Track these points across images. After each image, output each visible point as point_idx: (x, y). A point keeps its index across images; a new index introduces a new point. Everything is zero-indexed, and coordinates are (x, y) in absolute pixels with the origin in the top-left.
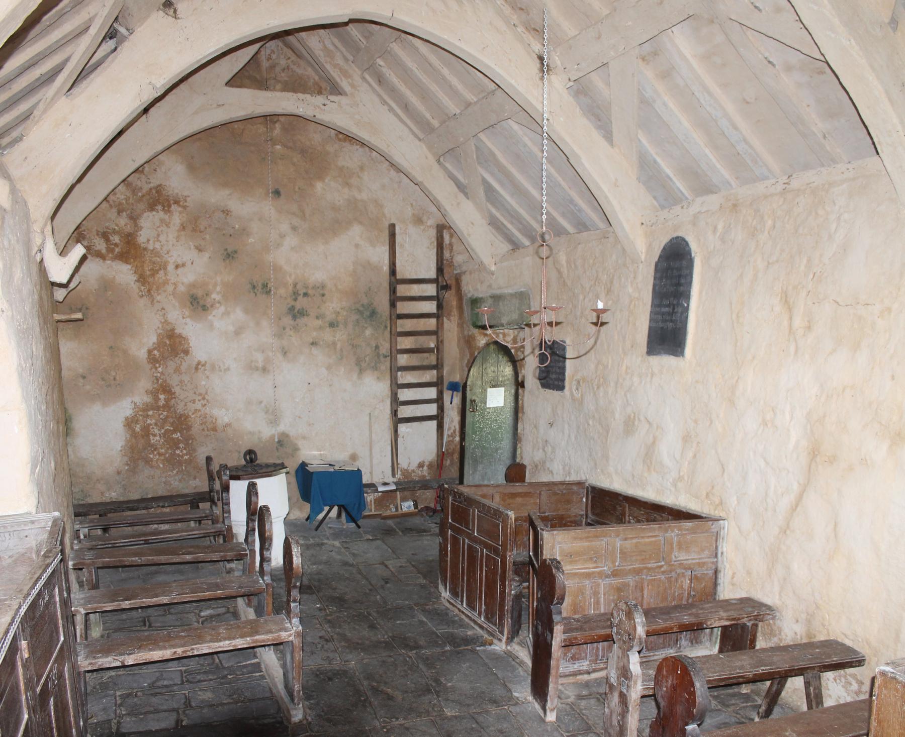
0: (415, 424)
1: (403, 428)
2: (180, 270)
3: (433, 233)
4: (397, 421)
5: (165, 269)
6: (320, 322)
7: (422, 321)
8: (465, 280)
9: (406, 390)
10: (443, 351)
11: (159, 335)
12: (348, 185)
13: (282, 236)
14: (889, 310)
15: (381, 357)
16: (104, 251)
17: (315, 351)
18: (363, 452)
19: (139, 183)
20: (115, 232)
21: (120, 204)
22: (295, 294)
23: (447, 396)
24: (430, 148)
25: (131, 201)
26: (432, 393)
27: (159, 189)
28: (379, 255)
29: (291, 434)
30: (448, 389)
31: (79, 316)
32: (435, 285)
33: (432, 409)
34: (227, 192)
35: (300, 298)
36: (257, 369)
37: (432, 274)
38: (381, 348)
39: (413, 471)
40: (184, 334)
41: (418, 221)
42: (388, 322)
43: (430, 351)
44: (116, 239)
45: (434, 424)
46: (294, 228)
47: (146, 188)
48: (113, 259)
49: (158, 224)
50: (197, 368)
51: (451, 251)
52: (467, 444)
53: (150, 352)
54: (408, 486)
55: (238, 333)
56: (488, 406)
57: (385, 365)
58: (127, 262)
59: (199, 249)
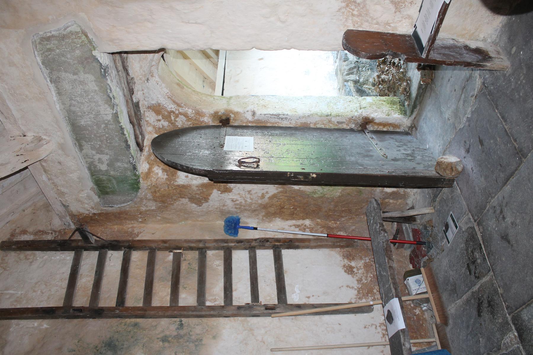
1: (294, 297)
4: (282, 305)
9: (234, 294)
10: (179, 241)
15: (182, 332)
23: (243, 234)
26: (241, 257)
30: (236, 233)
32: (85, 253)
33: (265, 257)
37: (68, 257)
38: (167, 333)
39: (359, 281)
42: (128, 320)
45: (286, 254)
51: (44, 232)
54: (388, 286)
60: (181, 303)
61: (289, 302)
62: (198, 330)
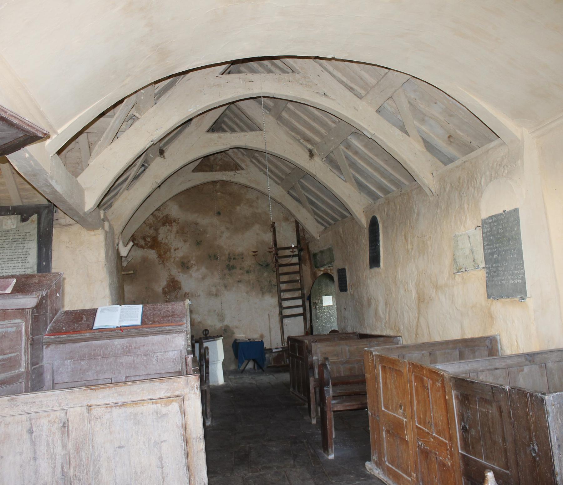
0: (292, 318)
1: (286, 321)
2: (176, 251)
3: (294, 224)
4: (282, 317)
5: (170, 251)
6: (242, 271)
7: (292, 267)
8: (311, 245)
9: (286, 302)
11: (167, 281)
12: (251, 206)
13: (222, 232)
14: (430, 237)
16: (144, 245)
17: (240, 285)
18: (266, 334)
19: (158, 215)
20: (148, 236)
21: (151, 224)
22: (229, 259)
24: (283, 188)
25: (155, 222)
26: (299, 302)
27: (167, 216)
28: (268, 237)
29: (230, 326)
31: (132, 272)
33: (300, 310)
34: (197, 215)
35: (232, 260)
36: (213, 295)
40: (179, 280)
41: (286, 219)
43: (296, 281)
44: (149, 239)
45: (302, 317)
46: (227, 228)
47: (161, 216)
48: (147, 248)
49: (166, 231)
50: (185, 296)
52: (313, 324)
53: (163, 289)
55: (204, 278)
56: (324, 305)
57: (275, 290)
58: (153, 249)
59: (185, 241)
60: (281, 285)
61: (284, 319)
62: (274, 291)
